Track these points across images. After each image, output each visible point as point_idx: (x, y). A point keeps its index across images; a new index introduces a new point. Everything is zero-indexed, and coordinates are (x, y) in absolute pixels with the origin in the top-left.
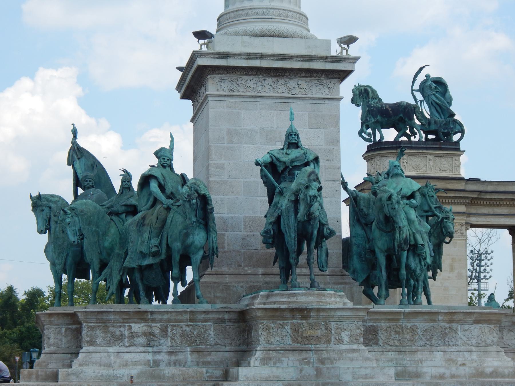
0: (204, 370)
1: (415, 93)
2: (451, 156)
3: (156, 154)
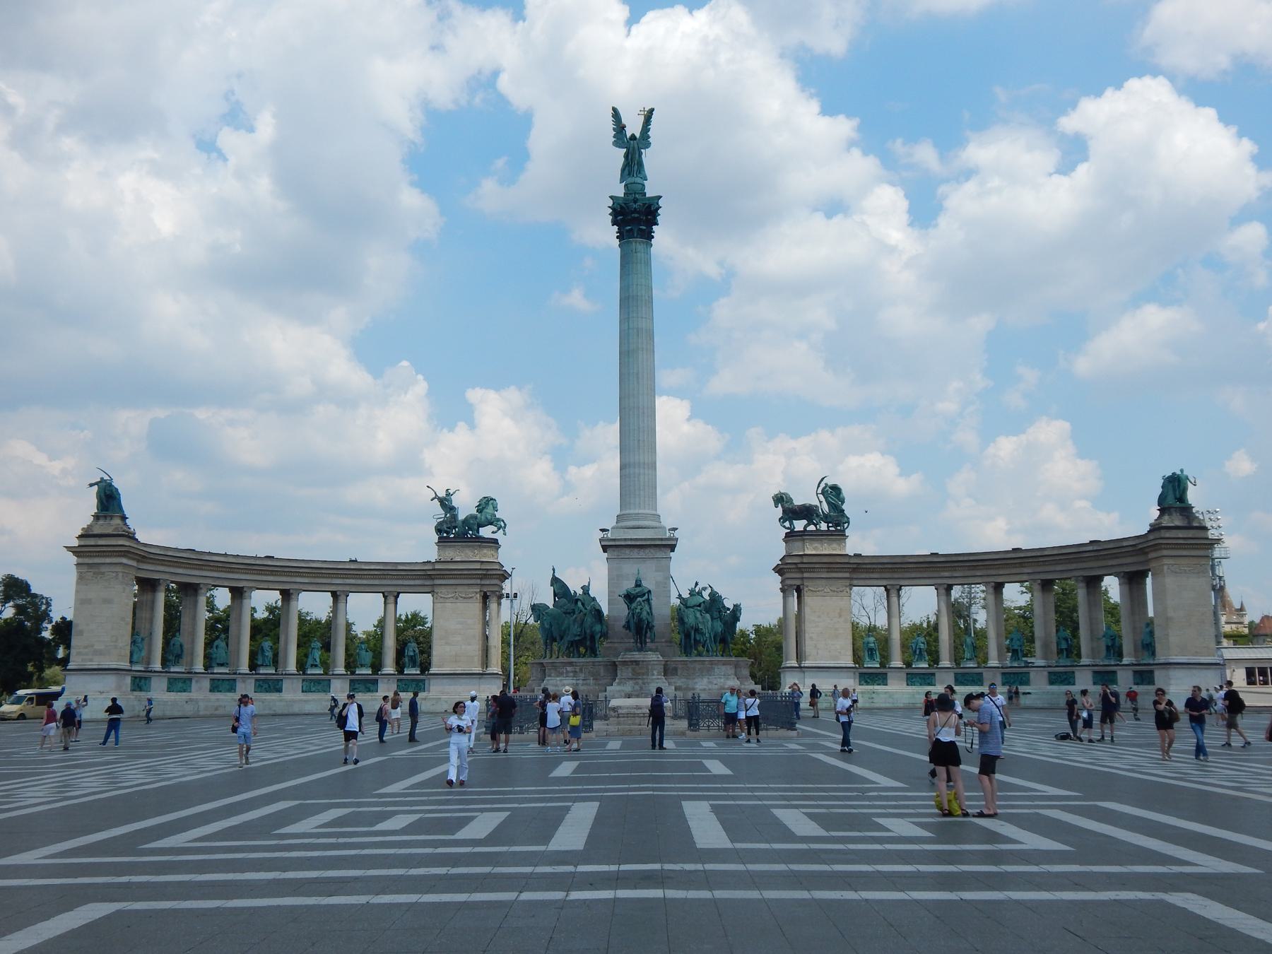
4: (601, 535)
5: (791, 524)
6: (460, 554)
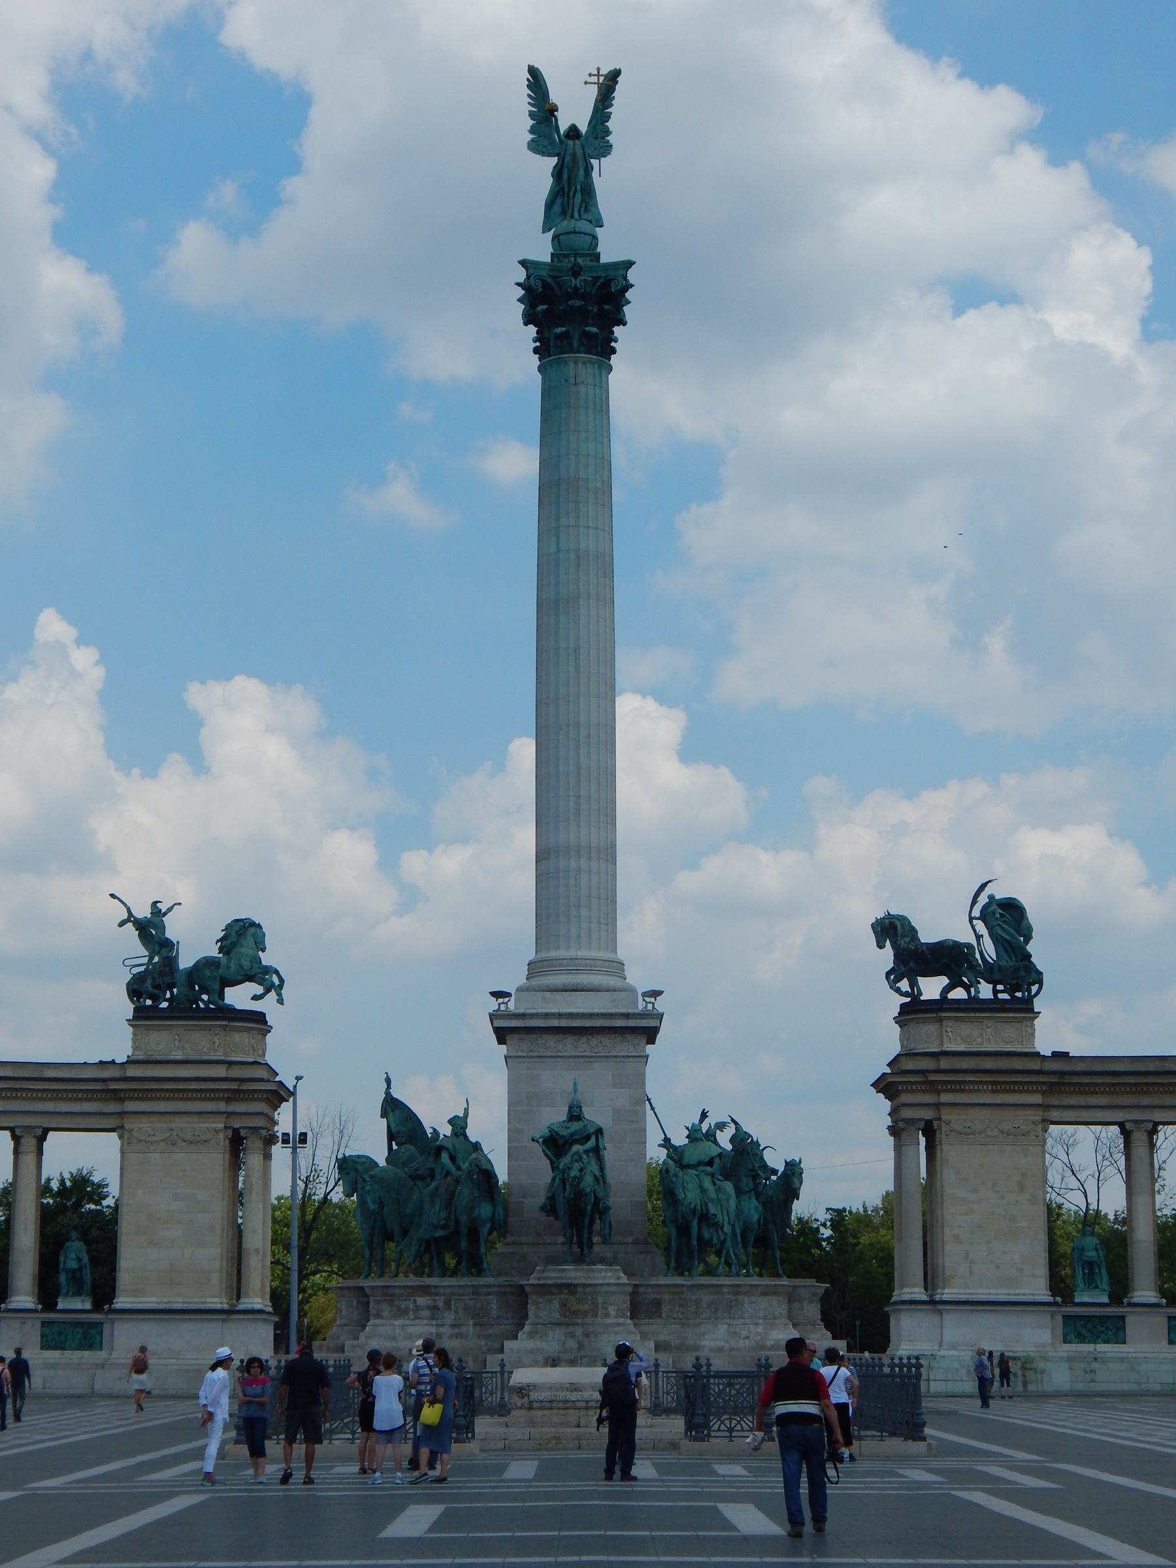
0: (483, 1343)
1: (975, 922)
2: (1020, 1021)
3: (450, 1122)
4: (493, 1004)
5: (913, 983)
6: (178, 1043)
